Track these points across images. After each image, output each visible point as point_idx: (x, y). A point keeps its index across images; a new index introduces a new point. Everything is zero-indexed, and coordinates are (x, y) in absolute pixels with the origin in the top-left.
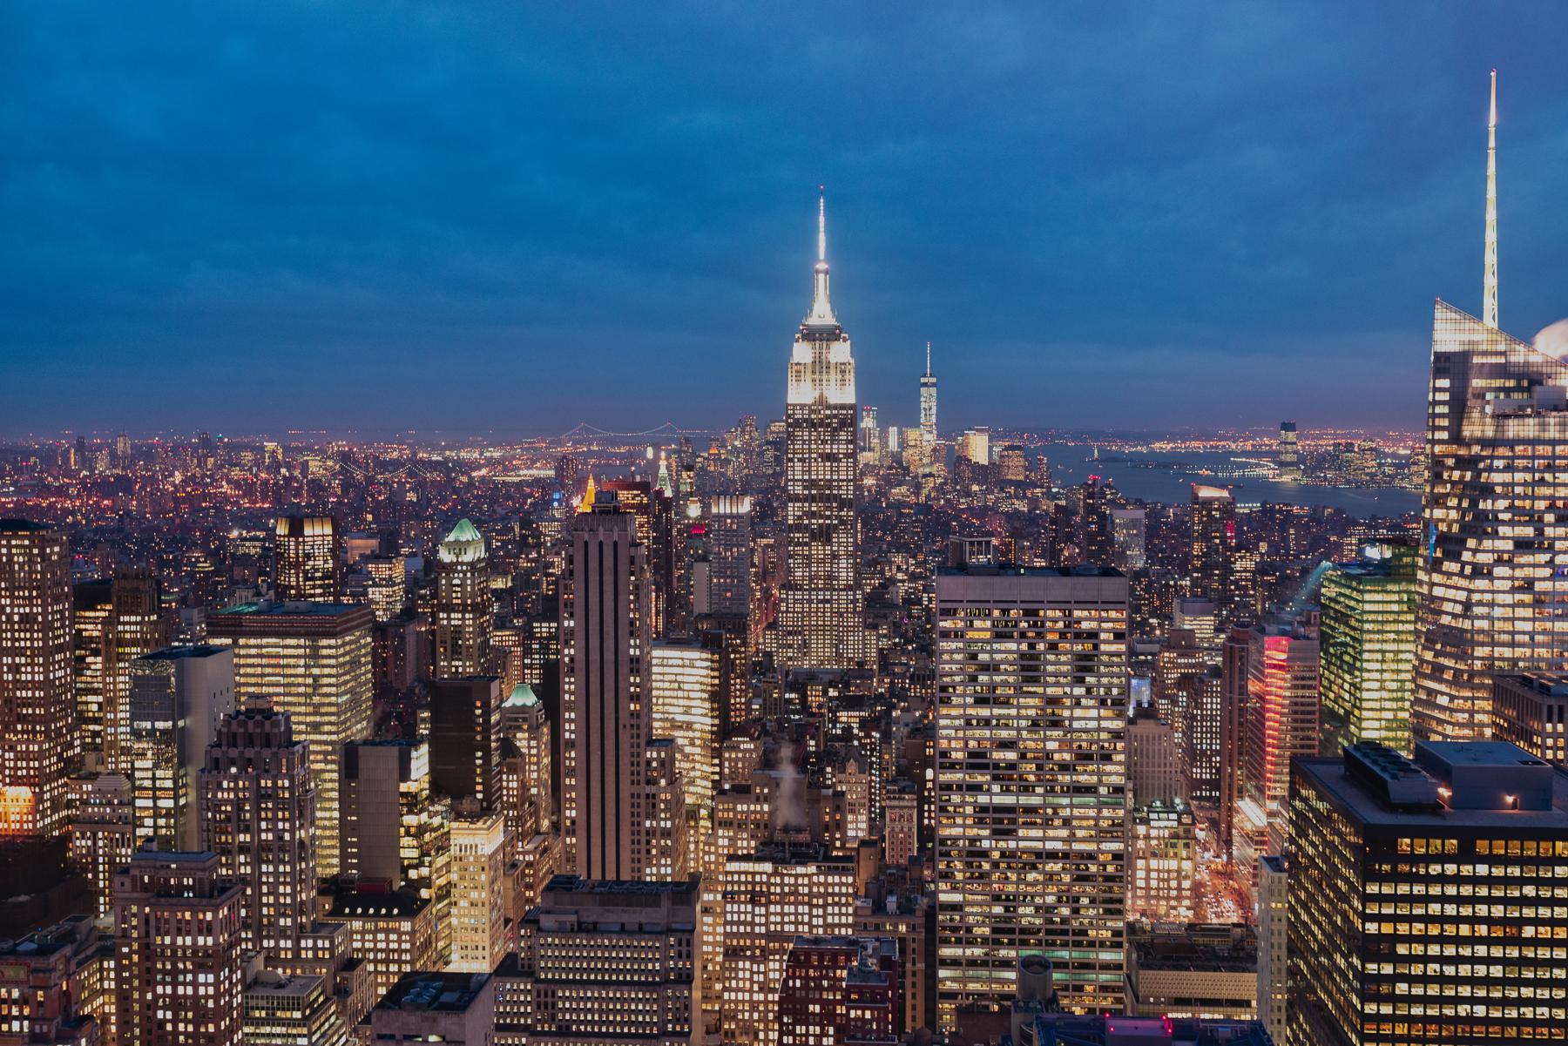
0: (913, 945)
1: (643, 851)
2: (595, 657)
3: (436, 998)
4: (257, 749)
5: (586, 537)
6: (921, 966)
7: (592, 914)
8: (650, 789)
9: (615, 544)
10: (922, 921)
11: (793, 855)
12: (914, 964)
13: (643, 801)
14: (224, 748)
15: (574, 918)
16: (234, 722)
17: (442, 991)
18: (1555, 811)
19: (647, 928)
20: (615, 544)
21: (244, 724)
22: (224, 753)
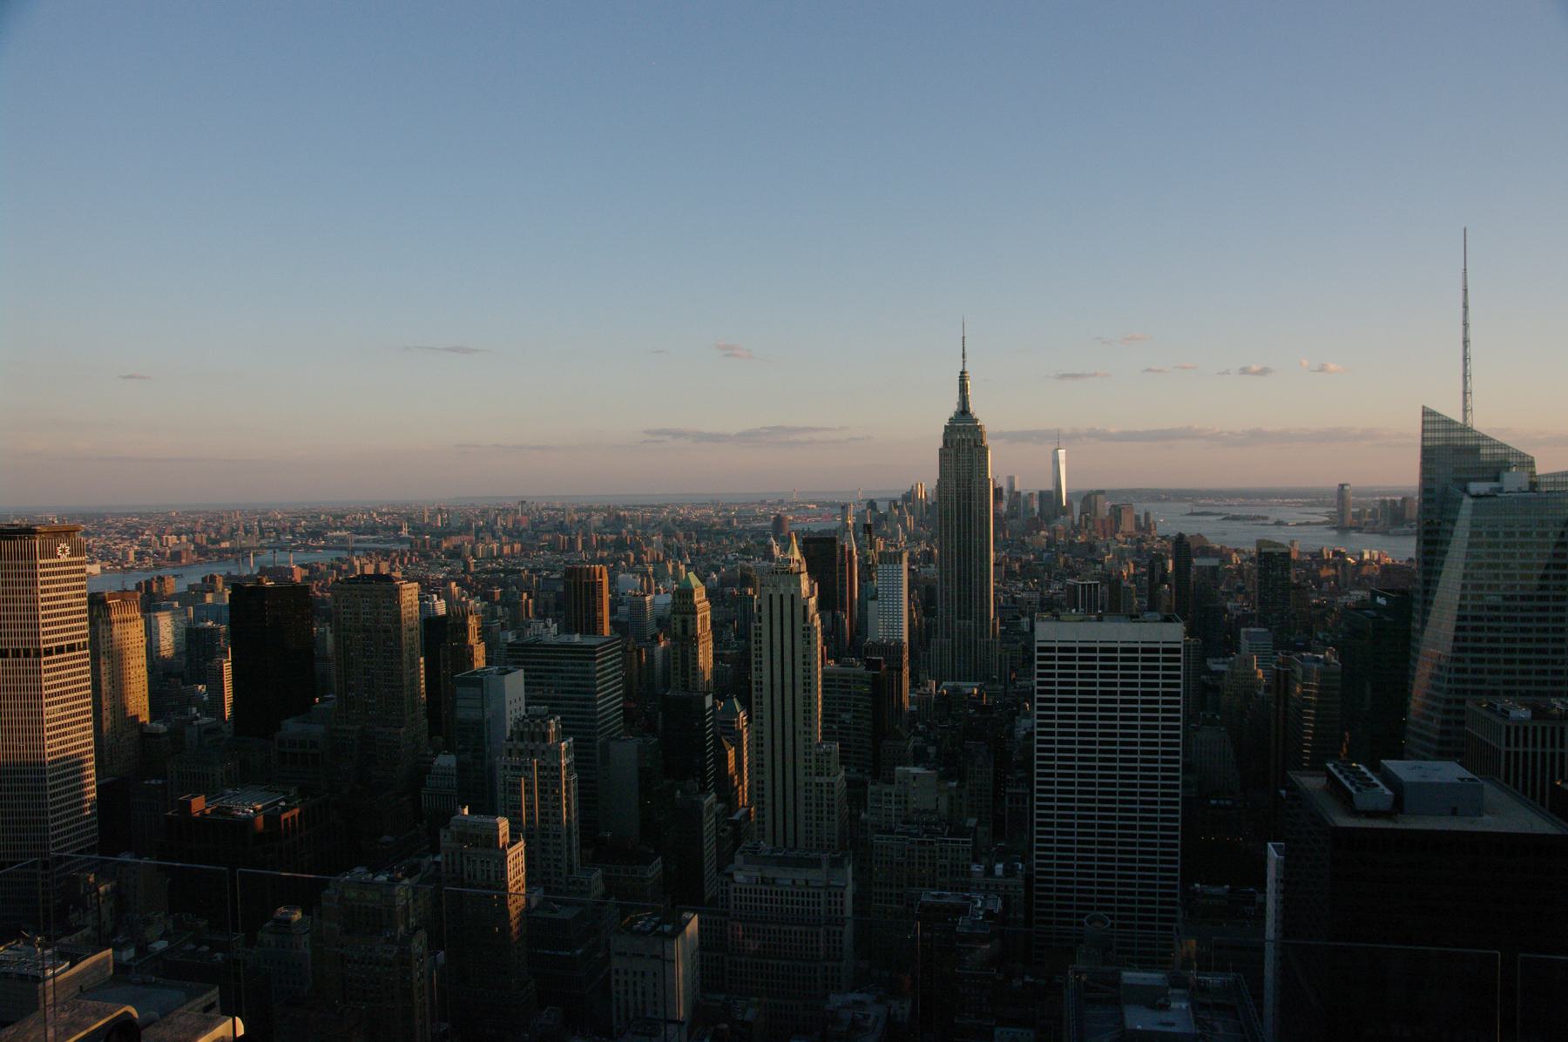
2: (777, 681)
3: (654, 928)
4: (538, 743)
5: (771, 591)
6: (1021, 916)
7: (770, 873)
8: (818, 780)
9: (792, 596)
11: (926, 831)
12: (1015, 915)
13: (813, 788)
14: (515, 742)
15: (759, 874)
16: (521, 725)
17: (659, 923)
18: (1486, 817)
19: (811, 884)
20: (792, 596)
21: (527, 725)
22: (515, 746)
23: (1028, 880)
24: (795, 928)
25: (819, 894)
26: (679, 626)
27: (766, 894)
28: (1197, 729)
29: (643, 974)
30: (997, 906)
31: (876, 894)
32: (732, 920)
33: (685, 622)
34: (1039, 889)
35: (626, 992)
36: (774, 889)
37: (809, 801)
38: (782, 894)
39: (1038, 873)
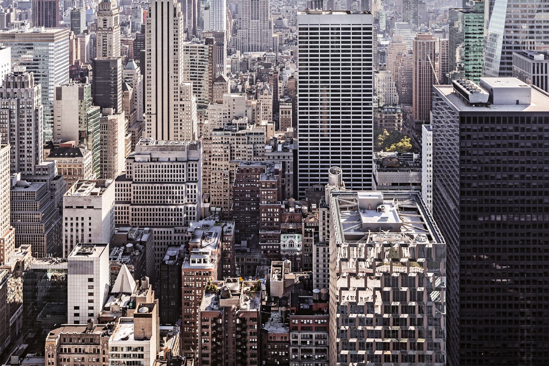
0: (288, 164)
1: (179, 128)
6: (291, 173)
10: (292, 154)
12: (289, 172)
23: (295, 152)
24: (170, 185)
25: (183, 166)
26: (102, 22)
27: (153, 167)
28: (377, 72)
29: (83, 219)
30: (278, 167)
31: (213, 164)
32: (133, 183)
33: (105, 20)
34: (300, 158)
35: (72, 230)
36: (158, 164)
37: (176, 115)
38: (162, 167)
39: (300, 149)
